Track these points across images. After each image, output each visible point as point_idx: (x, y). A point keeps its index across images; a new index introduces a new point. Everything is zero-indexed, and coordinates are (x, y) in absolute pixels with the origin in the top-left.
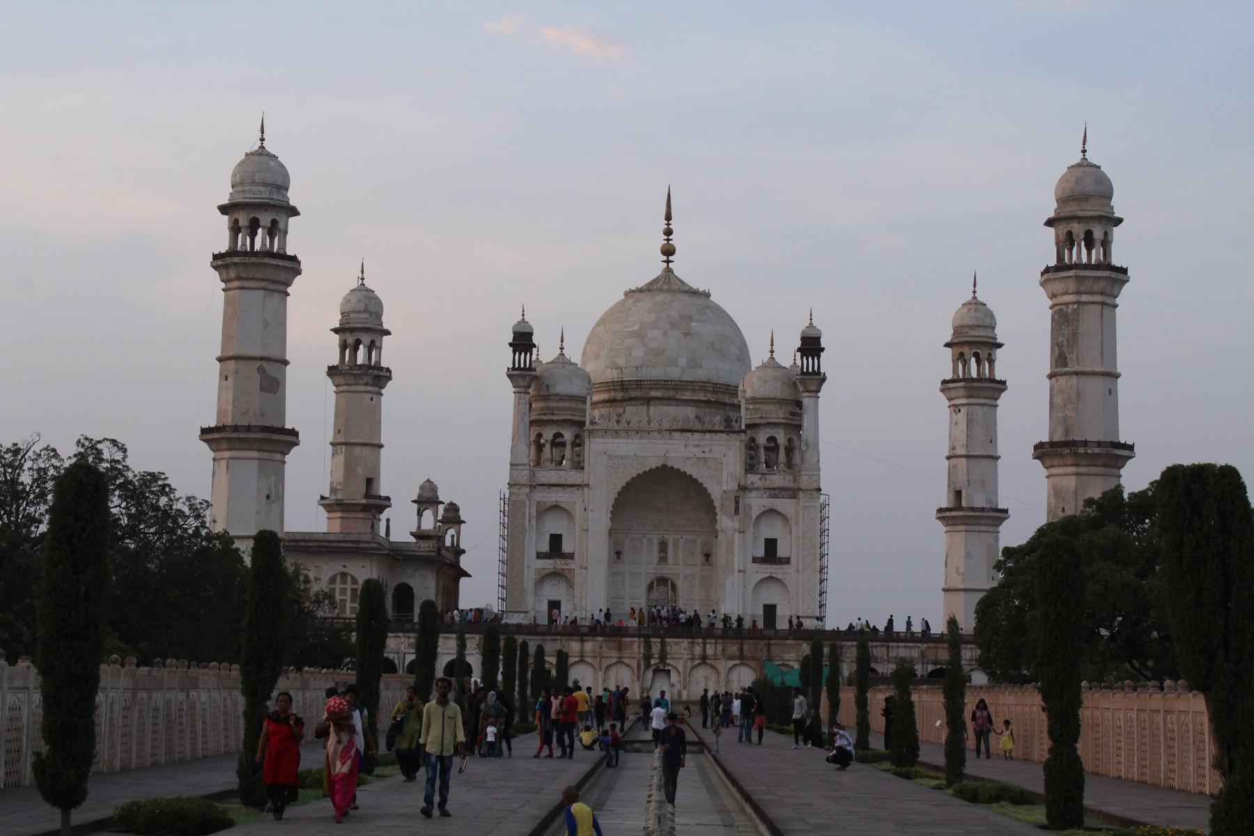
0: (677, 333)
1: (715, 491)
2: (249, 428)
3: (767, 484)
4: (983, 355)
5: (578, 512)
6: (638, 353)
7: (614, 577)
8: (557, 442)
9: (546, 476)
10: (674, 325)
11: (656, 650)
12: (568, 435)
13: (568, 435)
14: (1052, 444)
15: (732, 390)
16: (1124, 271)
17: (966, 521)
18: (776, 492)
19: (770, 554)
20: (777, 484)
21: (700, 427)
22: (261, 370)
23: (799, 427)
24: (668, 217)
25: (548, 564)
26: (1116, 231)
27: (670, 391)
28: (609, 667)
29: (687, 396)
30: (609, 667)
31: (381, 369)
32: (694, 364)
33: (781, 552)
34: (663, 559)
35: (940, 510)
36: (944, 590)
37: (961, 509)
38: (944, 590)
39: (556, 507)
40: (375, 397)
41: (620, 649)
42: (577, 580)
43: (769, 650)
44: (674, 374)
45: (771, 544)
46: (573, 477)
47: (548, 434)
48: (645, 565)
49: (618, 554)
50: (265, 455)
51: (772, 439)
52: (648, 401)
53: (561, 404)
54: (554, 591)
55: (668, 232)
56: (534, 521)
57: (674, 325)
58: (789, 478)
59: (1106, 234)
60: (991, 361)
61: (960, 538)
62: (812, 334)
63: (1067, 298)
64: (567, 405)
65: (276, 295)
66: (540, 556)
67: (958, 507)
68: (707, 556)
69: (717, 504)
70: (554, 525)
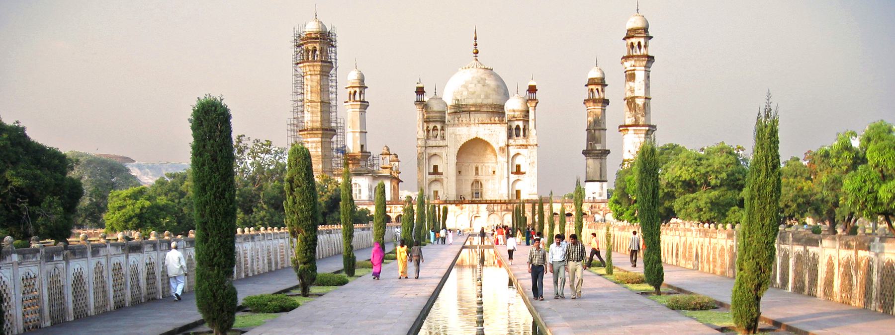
0: (480, 85)
1: (496, 148)
4: (600, 90)
7: (459, 181)
8: (435, 129)
9: (432, 142)
10: (479, 82)
11: (475, 210)
12: (439, 127)
13: (439, 127)
15: (502, 107)
16: (653, 57)
19: (518, 171)
24: (476, 39)
25: (433, 177)
26: (650, 41)
27: (478, 109)
29: (485, 109)
32: (487, 97)
33: (522, 170)
34: (477, 173)
42: (445, 183)
44: (479, 101)
45: (518, 167)
46: (442, 143)
47: (431, 126)
48: (472, 176)
52: (469, 112)
54: (436, 187)
57: (479, 82)
60: (602, 91)
62: (533, 83)
66: (430, 174)
69: (497, 152)
70: (434, 162)
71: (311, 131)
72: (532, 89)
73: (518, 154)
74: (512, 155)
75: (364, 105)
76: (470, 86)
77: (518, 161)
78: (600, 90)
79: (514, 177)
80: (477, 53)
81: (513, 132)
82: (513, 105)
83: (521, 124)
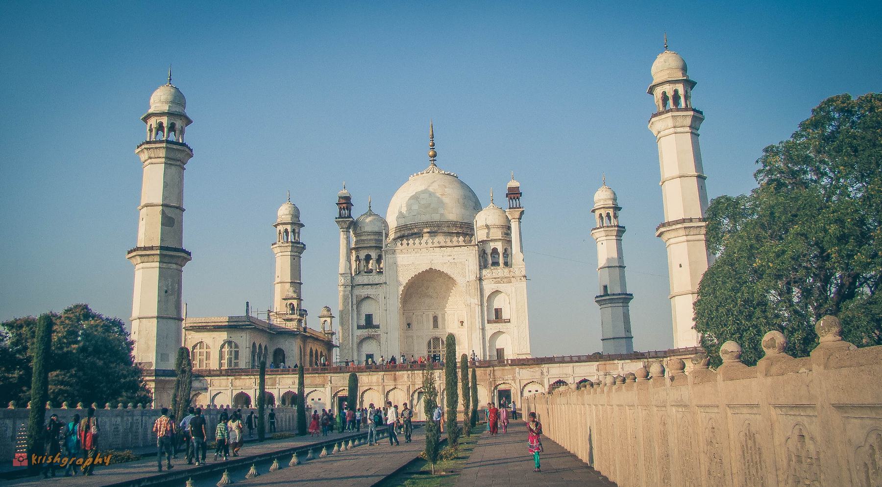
2: (152, 248)
3: (495, 275)
4: (612, 215)
5: (381, 299)
6: (415, 207)
9: (360, 279)
12: (374, 255)
13: (374, 255)
14: (669, 224)
17: (611, 301)
18: (498, 280)
20: (500, 275)
21: (449, 244)
22: (163, 213)
23: (510, 242)
25: (365, 332)
28: (388, 392)
29: (446, 229)
30: (388, 392)
31: (299, 243)
33: (505, 315)
35: (597, 297)
36: (603, 340)
37: (608, 295)
38: (603, 340)
39: (368, 297)
40: (296, 258)
41: (395, 380)
43: (494, 375)
45: (498, 312)
47: (363, 254)
48: (426, 332)
49: (409, 325)
50: (164, 265)
51: (495, 251)
53: (369, 237)
55: (433, 145)
56: (355, 307)
58: (506, 270)
59: (686, 92)
60: (616, 217)
61: (608, 310)
62: (514, 184)
63: (667, 132)
64: (372, 237)
65: (173, 167)
66: (359, 327)
67: (606, 294)
68: (462, 322)
70: (366, 308)
71: (144, 252)
72: (514, 194)
73: (497, 292)
74: (487, 293)
75: (298, 248)
76: (422, 196)
77: (496, 304)
78: (612, 215)
79: (491, 329)
80: (435, 156)
81: (487, 259)
82: (487, 219)
83: (499, 246)
